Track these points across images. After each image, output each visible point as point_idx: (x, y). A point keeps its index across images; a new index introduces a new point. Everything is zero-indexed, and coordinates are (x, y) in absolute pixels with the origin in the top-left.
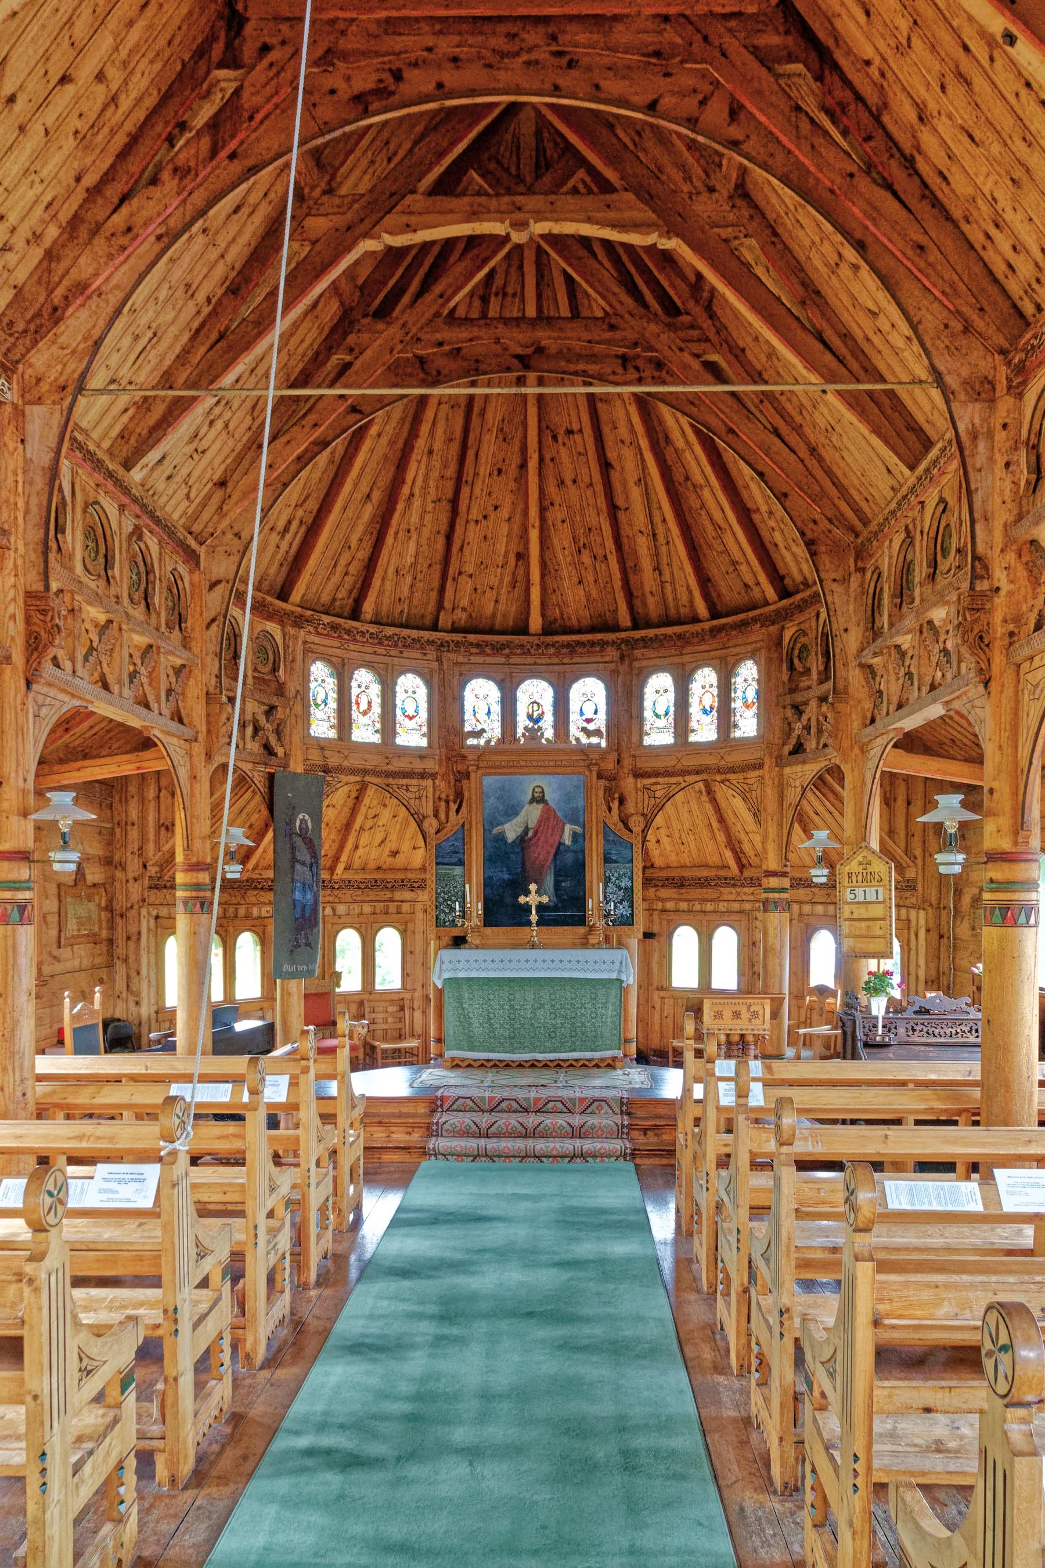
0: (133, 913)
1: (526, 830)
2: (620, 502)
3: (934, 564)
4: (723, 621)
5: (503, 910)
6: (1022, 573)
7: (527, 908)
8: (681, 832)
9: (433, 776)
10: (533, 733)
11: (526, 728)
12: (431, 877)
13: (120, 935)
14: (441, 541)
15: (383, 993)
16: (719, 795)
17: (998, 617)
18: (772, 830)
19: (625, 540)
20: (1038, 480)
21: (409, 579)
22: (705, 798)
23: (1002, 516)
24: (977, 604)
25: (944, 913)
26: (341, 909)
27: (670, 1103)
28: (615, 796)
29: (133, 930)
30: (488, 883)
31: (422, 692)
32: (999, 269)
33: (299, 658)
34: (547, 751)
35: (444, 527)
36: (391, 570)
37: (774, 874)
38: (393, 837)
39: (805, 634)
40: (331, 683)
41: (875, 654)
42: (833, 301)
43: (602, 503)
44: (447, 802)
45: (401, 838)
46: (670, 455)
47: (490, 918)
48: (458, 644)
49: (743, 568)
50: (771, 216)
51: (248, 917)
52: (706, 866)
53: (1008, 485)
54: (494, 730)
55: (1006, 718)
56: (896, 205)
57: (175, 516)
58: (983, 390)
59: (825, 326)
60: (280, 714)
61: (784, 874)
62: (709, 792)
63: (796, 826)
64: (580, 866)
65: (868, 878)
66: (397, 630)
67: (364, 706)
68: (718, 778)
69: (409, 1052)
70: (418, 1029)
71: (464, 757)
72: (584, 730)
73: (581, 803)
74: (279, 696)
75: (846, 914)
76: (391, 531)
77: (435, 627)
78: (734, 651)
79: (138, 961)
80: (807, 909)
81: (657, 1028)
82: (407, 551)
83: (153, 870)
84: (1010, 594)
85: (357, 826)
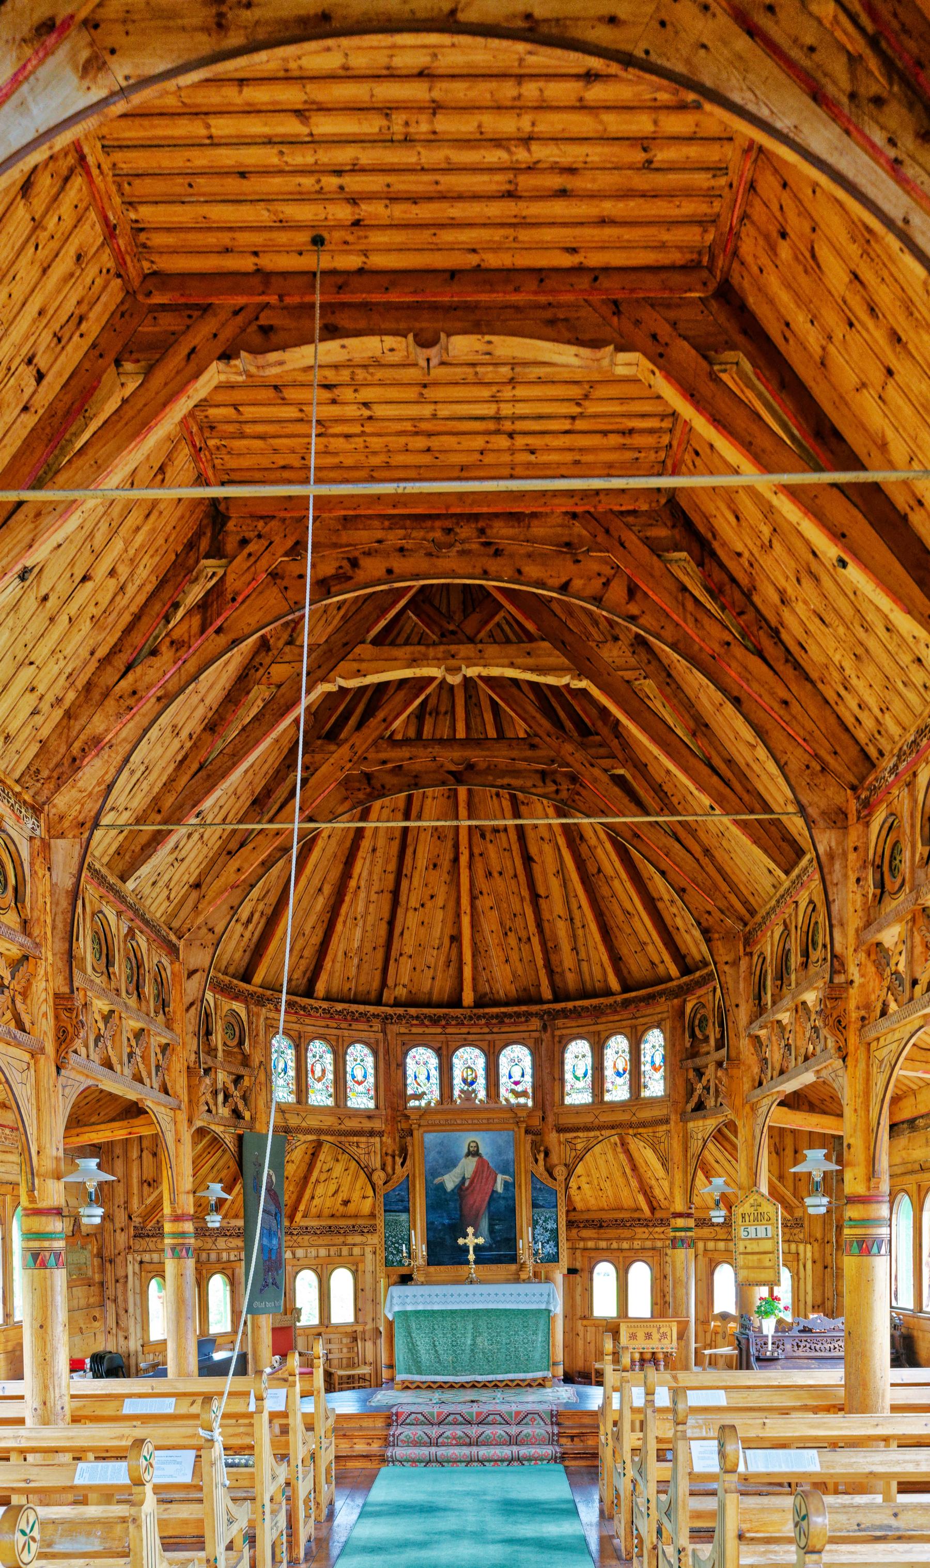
0: (119, 1260)
2: (542, 891)
3: (806, 954)
5: (444, 1252)
6: (871, 969)
7: (465, 1249)
8: (599, 1179)
10: (468, 1096)
11: (462, 1091)
12: (380, 1223)
13: (110, 1277)
14: (384, 927)
15: (337, 1326)
16: (632, 1147)
17: (852, 1004)
18: (678, 1176)
19: (546, 925)
20: (882, 893)
21: (356, 961)
22: (619, 1149)
23: (854, 922)
24: (835, 993)
25: (828, 1247)
26: (300, 1253)
27: (594, 1414)
28: (541, 1149)
29: (120, 1273)
30: (430, 1227)
32: (850, 721)
33: (262, 1033)
35: (386, 916)
36: (340, 954)
37: (680, 1215)
38: (345, 1188)
39: (704, 1006)
40: (290, 1054)
41: (761, 1028)
42: (720, 734)
43: (525, 893)
45: (352, 1189)
46: (584, 849)
47: (433, 1259)
48: (400, 1017)
49: (650, 949)
50: (666, 662)
51: (219, 1260)
52: (620, 1209)
53: (859, 898)
54: (432, 1092)
55: (860, 1087)
56: (764, 668)
58: (838, 819)
59: (714, 754)
60: (246, 1082)
61: (689, 1215)
63: (699, 1173)
65: (759, 1218)
66: (346, 1006)
68: (631, 1131)
69: (362, 1378)
70: (370, 1358)
71: (407, 1117)
72: (513, 1091)
73: (511, 1156)
74: (248, 1068)
75: (742, 1249)
76: (341, 919)
77: (379, 1002)
78: (642, 1020)
79: (126, 1301)
80: (711, 1245)
81: (581, 1352)
82: (355, 934)
83: (137, 1220)
84: (862, 985)
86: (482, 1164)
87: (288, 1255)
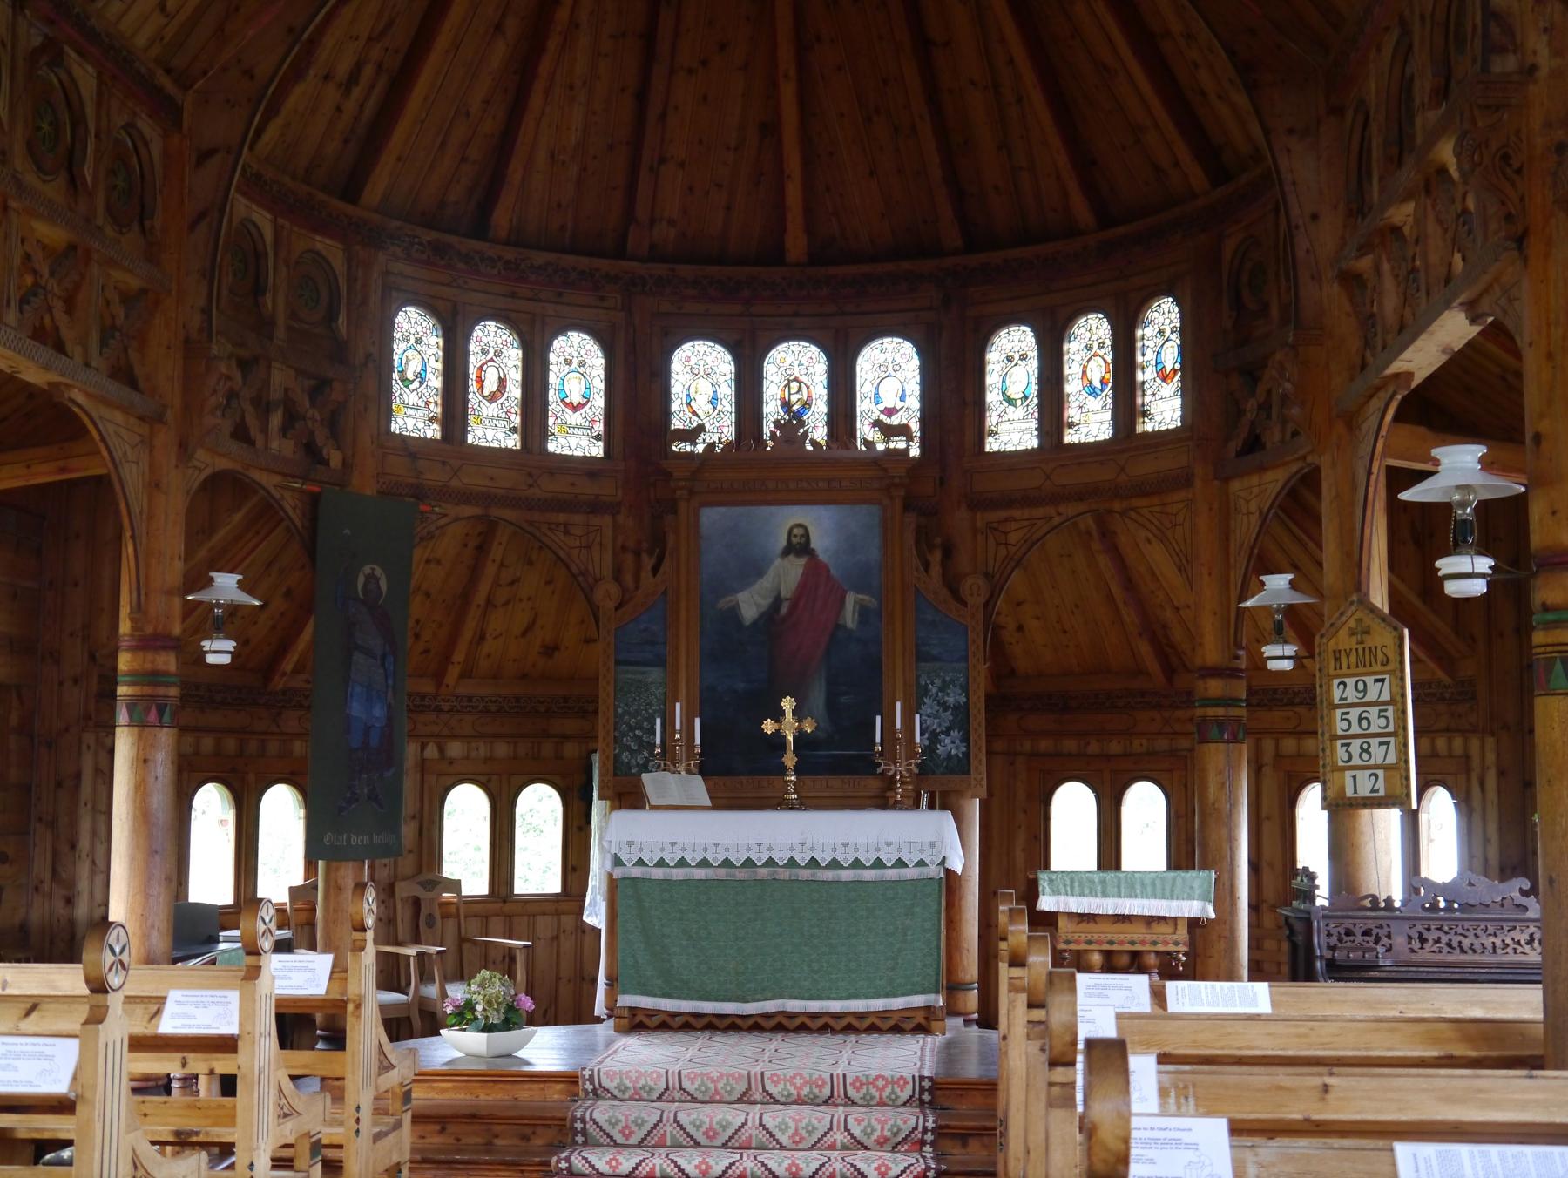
1: (778, 601)
4: (1121, 230)
9: (612, 509)
11: (776, 423)
22: (1096, 545)
31: (597, 362)
34: (818, 460)
40: (434, 344)
44: (638, 554)
54: (722, 428)
57: (141, 41)
62: (1107, 535)
64: (874, 667)
66: (552, 256)
67: (491, 385)
68: (1117, 506)
85: (480, 597)
86: (815, 569)
87: (411, 750)
